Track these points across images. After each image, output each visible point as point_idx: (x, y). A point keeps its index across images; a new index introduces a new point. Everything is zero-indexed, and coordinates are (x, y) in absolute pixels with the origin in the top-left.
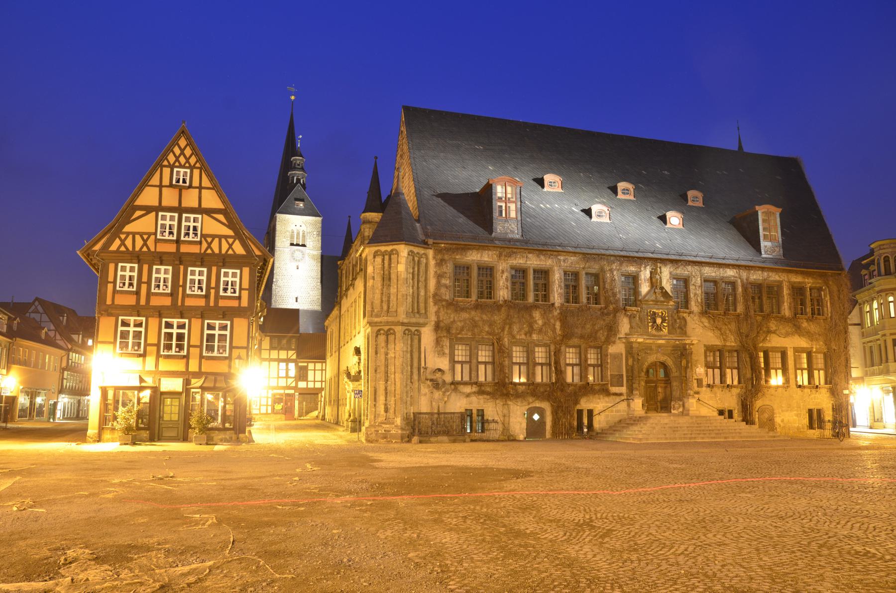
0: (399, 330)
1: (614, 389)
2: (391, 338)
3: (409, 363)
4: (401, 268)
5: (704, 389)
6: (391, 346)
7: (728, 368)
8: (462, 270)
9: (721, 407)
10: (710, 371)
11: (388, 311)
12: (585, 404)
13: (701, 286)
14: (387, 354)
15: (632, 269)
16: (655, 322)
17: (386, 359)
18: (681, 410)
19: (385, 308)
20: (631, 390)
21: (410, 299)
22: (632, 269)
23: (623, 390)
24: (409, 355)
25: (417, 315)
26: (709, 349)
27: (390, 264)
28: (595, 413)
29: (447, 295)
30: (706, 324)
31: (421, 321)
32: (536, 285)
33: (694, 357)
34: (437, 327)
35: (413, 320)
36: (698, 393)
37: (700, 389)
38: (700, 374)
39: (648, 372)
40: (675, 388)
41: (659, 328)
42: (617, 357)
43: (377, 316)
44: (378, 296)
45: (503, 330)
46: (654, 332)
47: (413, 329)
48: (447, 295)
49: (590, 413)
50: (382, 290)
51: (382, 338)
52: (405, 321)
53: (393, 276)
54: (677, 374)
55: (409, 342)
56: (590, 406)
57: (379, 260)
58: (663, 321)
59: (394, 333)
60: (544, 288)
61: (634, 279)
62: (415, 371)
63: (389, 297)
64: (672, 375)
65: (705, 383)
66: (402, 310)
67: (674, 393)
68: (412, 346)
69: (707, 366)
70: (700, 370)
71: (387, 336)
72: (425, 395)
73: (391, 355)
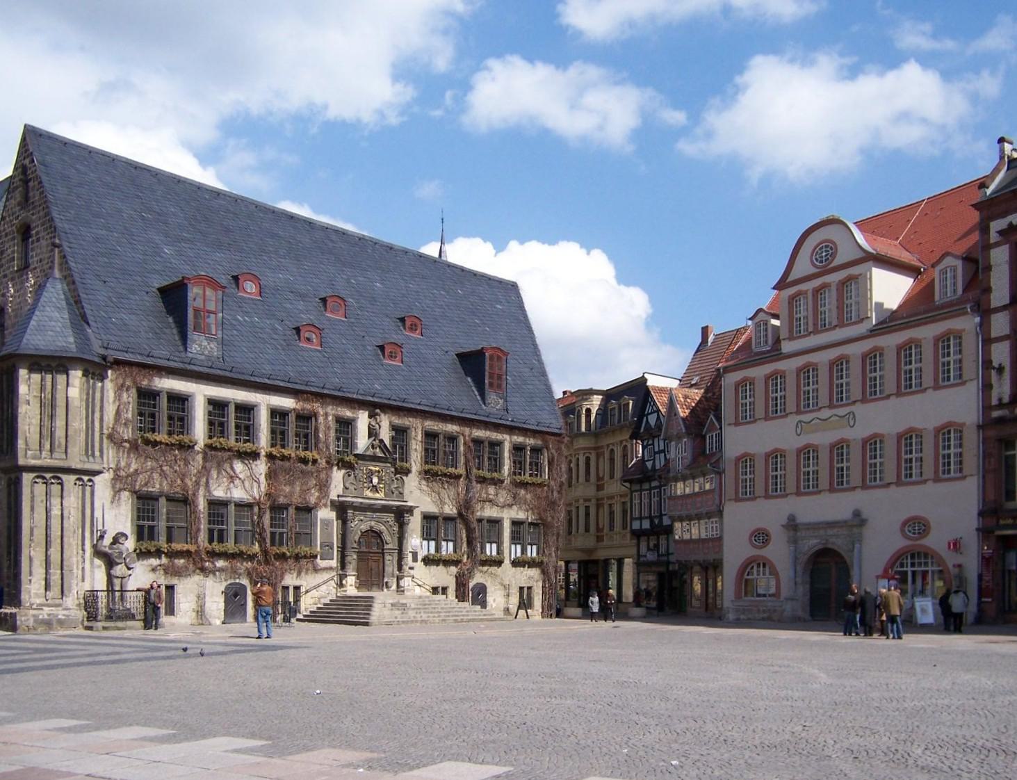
1: (322, 563)
2: (55, 489)
4: (74, 392)
6: (56, 501)
7: (444, 540)
8: (147, 396)
9: (435, 583)
10: (425, 543)
11: (51, 451)
12: (290, 580)
13: (422, 442)
14: (48, 511)
15: (348, 413)
16: (372, 482)
17: (48, 518)
19: (48, 446)
20: (343, 565)
22: (348, 413)
23: (334, 563)
25: (91, 458)
26: (428, 518)
28: (303, 589)
29: (127, 433)
30: (425, 488)
31: (96, 467)
32: (237, 427)
34: (117, 478)
35: (88, 466)
36: (411, 568)
37: (415, 564)
40: (387, 562)
41: (375, 489)
42: (327, 523)
43: (34, 458)
44: (35, 430)
45: (197, 483)
47: (86, 478)
48: (127, 433)
49: (297, 588)
51: (40, 488)
52: (79, 466)
53: (61, 402)
54: (390, 546)
56: (297, 583)
59: (61, 484)
60: (247, 430)
61: (346, 426)
65: (420, 558)
67: (386, 568)
72: (100, 567)
73: (56, 512)
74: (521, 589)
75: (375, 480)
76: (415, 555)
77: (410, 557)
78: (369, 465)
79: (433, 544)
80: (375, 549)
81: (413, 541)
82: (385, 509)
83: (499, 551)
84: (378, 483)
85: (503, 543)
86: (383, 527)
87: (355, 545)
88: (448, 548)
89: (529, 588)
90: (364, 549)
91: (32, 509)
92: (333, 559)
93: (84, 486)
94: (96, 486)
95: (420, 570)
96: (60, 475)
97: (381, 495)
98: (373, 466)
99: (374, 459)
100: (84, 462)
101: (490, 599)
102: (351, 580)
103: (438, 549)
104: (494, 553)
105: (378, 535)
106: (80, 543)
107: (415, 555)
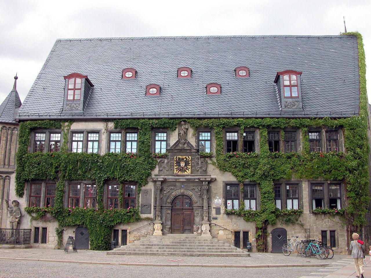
5: (221, 216)
9: (237, 229)
18: (199, 231)
25: (7, 167)
26: (227, 184)
28: (128, 231)
36: (216, 219)
37: (218, 216)
39: (173, 202)
41: (182, 170)
46: (180, 173)
47: (4, 176)
49: (124, 232)
58: (187, 163)
62: (5, 202)
64: (195, 205)
65: (222, 211)
70: (218, 201)
75: (183, 164)
76: (218, 211)
77: (213, 212)
78: (178, 155)
79: (236, 202)
80: (187, 206)
81: (216, 201)
82: (189, 181)
84: (186, 165)
86: (191, 193)
87: (170, 205)
88: (251, 205)
89: (333, 232)
90: (178, 207)
92: (150, 213)
94: (11, 179)
95: (222, 220)
97: (189, 172)
98: (182, 155)
99: (182, 151)
102: (158, 226)
103: (242, 205)
104: (296, 207)
105: (189, 198)
107: (218, 211)
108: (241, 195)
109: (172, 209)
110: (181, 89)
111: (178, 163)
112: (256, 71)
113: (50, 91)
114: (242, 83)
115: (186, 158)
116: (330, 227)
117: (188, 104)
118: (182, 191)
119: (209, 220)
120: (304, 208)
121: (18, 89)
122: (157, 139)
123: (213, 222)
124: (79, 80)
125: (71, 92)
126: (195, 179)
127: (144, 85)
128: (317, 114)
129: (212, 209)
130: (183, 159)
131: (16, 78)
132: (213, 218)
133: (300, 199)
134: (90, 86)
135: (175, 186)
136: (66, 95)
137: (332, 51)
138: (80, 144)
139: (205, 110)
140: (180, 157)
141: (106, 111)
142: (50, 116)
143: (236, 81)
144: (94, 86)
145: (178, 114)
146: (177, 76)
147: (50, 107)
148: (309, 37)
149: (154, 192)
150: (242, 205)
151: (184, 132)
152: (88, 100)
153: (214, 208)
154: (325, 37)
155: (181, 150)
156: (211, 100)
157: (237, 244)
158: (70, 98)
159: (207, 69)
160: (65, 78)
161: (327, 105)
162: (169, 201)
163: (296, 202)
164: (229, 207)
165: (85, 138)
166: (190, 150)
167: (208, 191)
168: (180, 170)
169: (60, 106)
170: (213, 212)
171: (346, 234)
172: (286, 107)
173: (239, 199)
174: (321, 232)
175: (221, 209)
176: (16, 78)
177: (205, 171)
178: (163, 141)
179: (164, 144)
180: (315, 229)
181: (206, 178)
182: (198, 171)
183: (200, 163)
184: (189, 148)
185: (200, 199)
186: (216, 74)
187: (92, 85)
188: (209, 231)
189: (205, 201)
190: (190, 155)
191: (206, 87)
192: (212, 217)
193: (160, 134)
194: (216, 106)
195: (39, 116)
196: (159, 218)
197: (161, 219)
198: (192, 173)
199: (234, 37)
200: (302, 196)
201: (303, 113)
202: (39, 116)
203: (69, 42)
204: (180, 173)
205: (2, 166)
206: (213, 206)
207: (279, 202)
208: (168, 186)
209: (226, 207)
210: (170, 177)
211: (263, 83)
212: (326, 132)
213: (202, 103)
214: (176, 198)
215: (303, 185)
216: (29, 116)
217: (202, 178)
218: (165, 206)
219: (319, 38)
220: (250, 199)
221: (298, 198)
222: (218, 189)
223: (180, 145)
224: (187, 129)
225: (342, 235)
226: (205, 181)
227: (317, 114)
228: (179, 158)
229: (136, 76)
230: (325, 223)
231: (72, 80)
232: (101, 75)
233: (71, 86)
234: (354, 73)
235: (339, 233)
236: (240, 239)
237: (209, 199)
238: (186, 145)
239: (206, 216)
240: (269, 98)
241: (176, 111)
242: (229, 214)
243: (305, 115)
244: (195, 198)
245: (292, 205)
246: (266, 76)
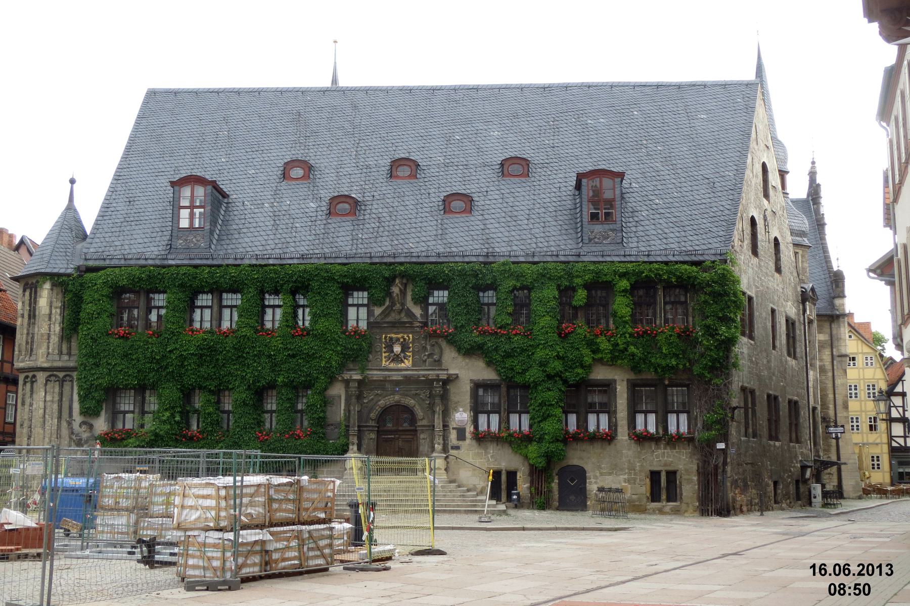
0: (41, 377)
3: (56, 414)
5: (468, 441)
6: (35, 396)
14: (31, 405)
16: (392, 351)
21: (55, 339)
24: (55, 406)
25: (66, 358)
26: (477, 386)
27: (35, 298)
33: (454, 397)
35: (60, 364)
36: (457, 448)
37: (461, 443)
38: (462, 421)
41: (397, 359)
43: (23, 361)
46: (392, 365)
47: (61, 375)
50: (28, 330)
52: (45, 365)
53: (37, 313)
54: (424, 422)
55: (57, 390)
57: (27, 293)
58: (404, 348)
62: (64, 424)
63: (33, 338)
66: (42, 351)
68: (61, 394)
69: (477, 409)
70: (462, 416)
71: (32, 383)
73: (34, 406)
74: (655, 476)
75: (397, 349)
77: (453, 435)
79: (495, 418)
80: (406, 426)
82: (408, 380)
83: (613, 426)
84: (403, 351)
85: (615, 412)
86: (412, 401)
88: (520, 423)
89: (672, 475)
90: (389, 425)
91: (23, 404)
93: (62, 382)
95: (468, 451)
96: (35, 373)
97: (408, 363)
99: (397, 325)
100: (54, 361)
101: (592, 487)
105: (409, 410)
106: (54, 432)
108: (504, 406)
109: (378, 431)
110: (396, 204)
111: (390, 348)
112: (544, 165)
113: (142, 206)
114: (513, 190)
115: (403, 337)
116: (665, 465)
117: (407, 236)
118: (397, 397)
119: (445, 450)
120: (619, 430)
121: (77, 204)
122: (350, 301)
123: (452, 452)
124: (200, 191)
125: (185, 213)
126: (419, 376)
127: (326, 194)
128: (648, 255)
129: (452, 431)
130: (398, 339)
131: (72, 181)
132: (453, 448)
133: (611, 411)
134: (221, 197)
135: (384, 389)
136: (176, 218)
137: (702, 116)
138: (207, 313)
139: (438, 247)
140: (393, 336)
141: (254, 249)
142: (146, 259)
143: (502, 187)
144: (228, 196)
145: (389, 256)
146: (391, 176)
147: (146, 240)
148: (658, 86)
149: (346, 400)
150: (505, 422)
151: (401, 290)
152: (219, 227)
153: (454, 428)
154: (693, 85)
155: (395, 323)
156: (452, 226)
157: (495, 494)
158: (184, 223)
159: (448, 161)
160: (173, 184)
161: (672, 235)
162: (373, 415)
163: (604, 418)
164: (483, 427)
165: (215, 301)
166: (411, 323)
167: (445, 397)
168: (393, 360)
169: (165, 238)
170: (453, 435)
171: (695, 478)
172: (590, 240)
173: (499, 412)
174: (648, 473)
175: (468, 430)
176: (72, 181)
177: (439, 362)
178: (363, 305)
179: (363, 312)
180: (638, 468)
181: (438, 375)
182: (425, 361)
183: (428, 347)
184: (409, 320)
185: (429, 412)
186: (465, 171)
187: (225, 195)
188: (446, 470)
189: (436, 416)
190: (411, 333)
191: (444, 201)
192: (450, 444)
193: (355, 294)
194: (461, 239)
195: (125, 259)
196: (355, 448)
197: (359, 449)
198: (413, 366)
199: (507, 88)
200: (616, 407)
201: (622, 253)
202: (125, 259)
203: (172, 96)
204: (392, 365)
205: (57, 357)
206: (453, 425)
207: (573, 419)
208: (371, 390)
209: (476, 427)
210: (375, 372)
211: (554, 190)
212: (664, 288)
213: (435, 233)
214: (386, 411)
215: (619, 388)
216: (104, 259)
217: (432, 374)
218: (367, 426)
219: (679, 86)
220: (520, 413)
221: (608, 412)
222: (462, 393)
223: (393, 314)
224: (406, 285)
225: (689, 481)
226: (438, 380)
227: (648, 255)
228: (391, 339)
229: (311, 176)
230: (657, 457)
231: (186, 192)
232: (241, 173)
233: (185, 202)
234: (735, 167)
235: (684, 477)
236: (502, 487)
237: (446, 414)
238: (403, 315)
239: (439, 444)
240: (560, 223)
241: (384, 248)
242: (481, 438)
243: (625, 256)
244: (419, 413)
245: (597, 422)
246: (561, 176)
